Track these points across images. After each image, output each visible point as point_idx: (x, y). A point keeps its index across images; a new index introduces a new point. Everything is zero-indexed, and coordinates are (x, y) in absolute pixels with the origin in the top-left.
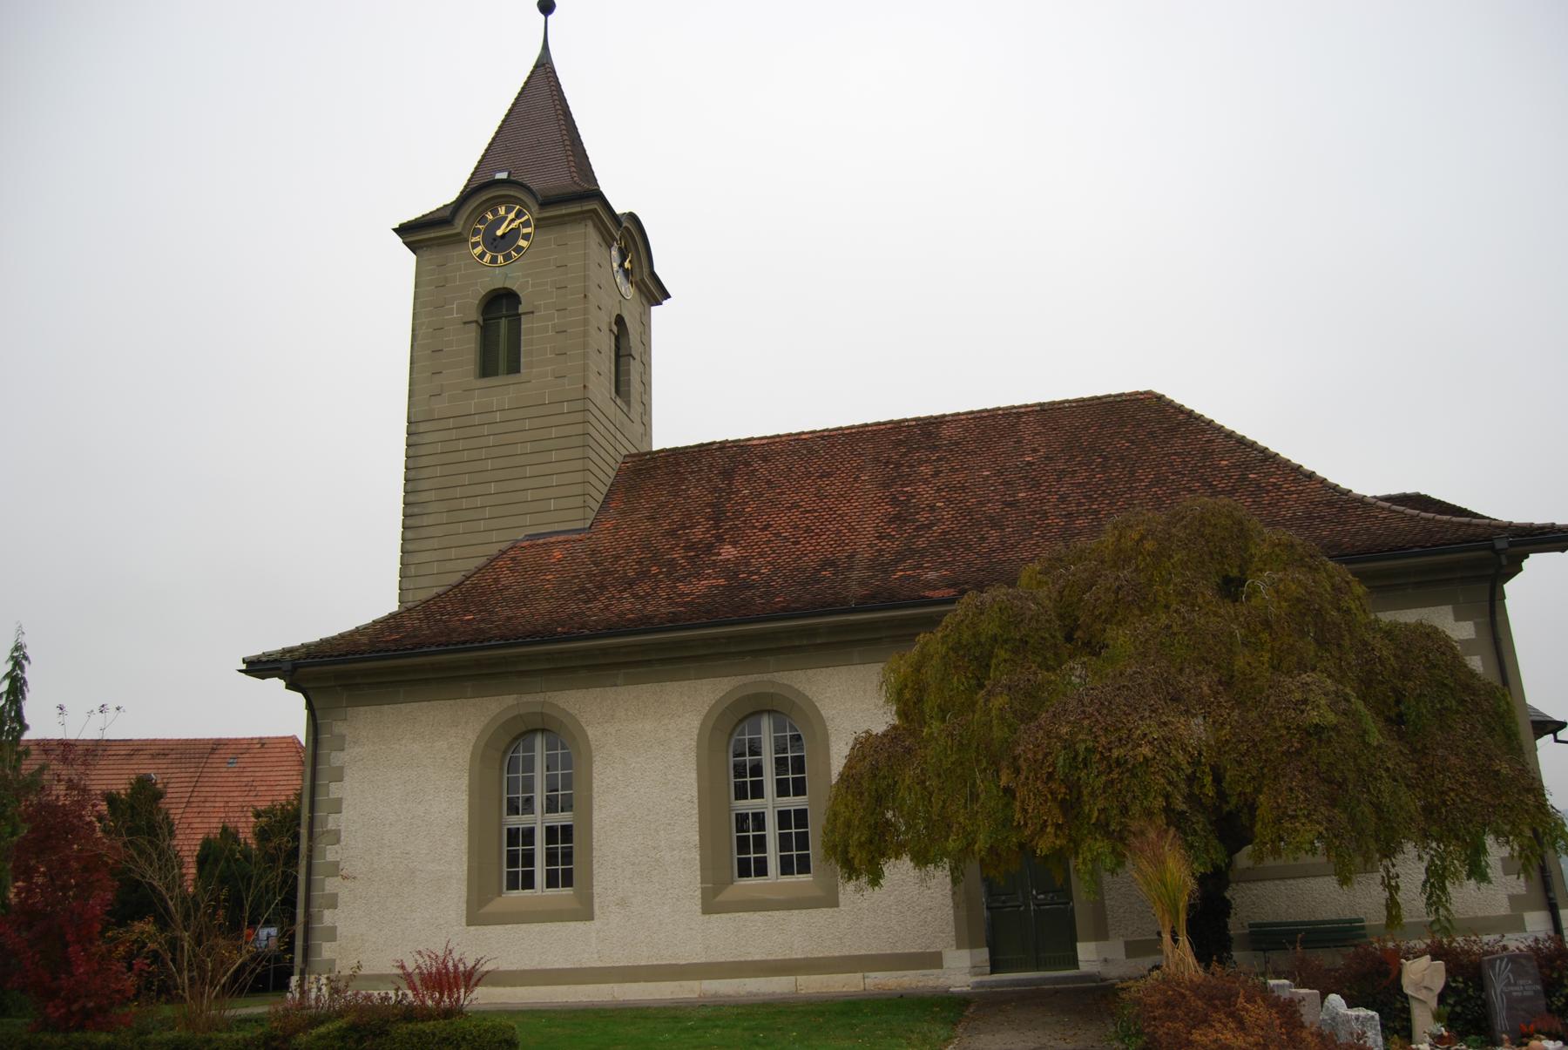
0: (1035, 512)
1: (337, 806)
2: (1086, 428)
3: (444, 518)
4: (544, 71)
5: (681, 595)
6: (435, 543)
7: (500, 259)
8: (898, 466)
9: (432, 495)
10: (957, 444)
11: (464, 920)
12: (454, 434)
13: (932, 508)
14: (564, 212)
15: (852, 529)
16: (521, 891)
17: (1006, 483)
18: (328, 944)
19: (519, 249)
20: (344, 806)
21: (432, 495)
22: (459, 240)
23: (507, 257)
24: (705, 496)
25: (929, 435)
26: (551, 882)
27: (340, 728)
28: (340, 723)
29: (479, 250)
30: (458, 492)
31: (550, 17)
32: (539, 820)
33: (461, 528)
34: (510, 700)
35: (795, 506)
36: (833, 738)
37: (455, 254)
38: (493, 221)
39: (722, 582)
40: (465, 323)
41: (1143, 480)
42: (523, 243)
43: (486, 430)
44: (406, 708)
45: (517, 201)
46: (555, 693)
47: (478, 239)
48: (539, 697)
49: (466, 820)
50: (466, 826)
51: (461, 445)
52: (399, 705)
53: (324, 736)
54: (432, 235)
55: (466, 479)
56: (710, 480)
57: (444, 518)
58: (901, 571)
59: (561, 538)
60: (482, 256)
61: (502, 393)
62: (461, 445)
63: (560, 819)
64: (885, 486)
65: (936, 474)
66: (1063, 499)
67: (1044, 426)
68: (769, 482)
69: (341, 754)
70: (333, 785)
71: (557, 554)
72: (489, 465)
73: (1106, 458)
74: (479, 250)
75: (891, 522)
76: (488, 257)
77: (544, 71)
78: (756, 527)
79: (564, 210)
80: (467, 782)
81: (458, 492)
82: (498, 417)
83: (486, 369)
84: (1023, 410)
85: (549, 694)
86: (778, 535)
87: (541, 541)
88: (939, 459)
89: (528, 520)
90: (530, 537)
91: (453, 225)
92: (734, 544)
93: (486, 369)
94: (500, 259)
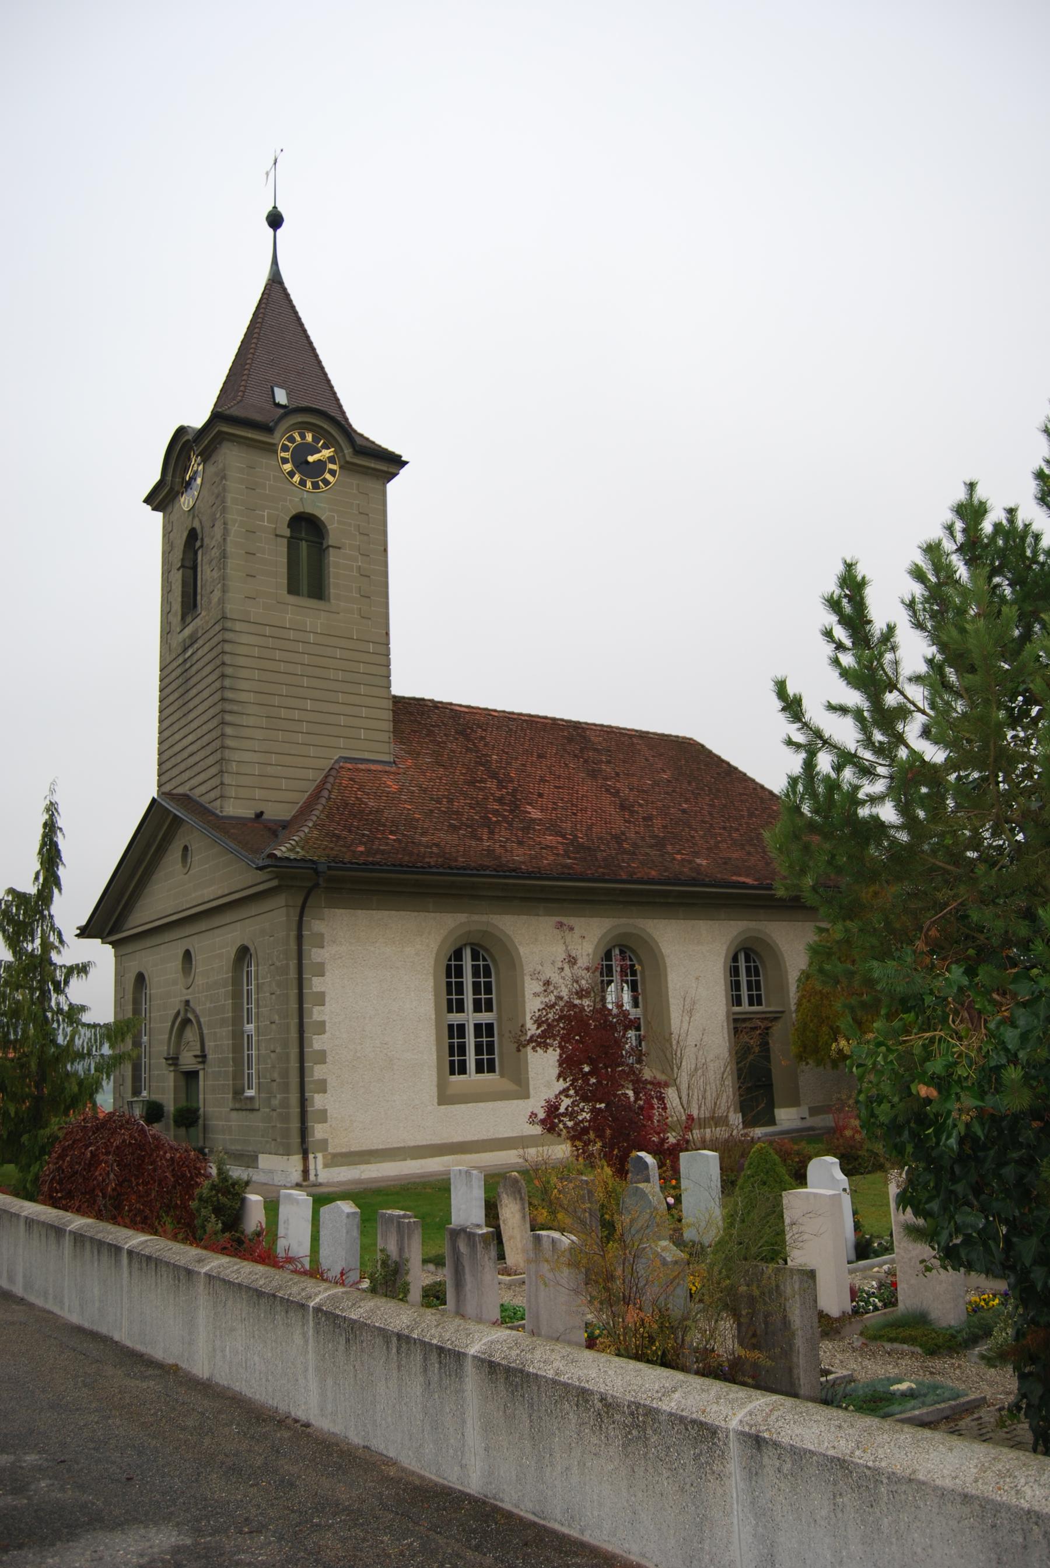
1: (320, 999)
3: (264, 722)
4: (275, 286)
7: (309, 484)
9: (251, 697)
11: (436, 1100)
14: (373, 465)
16: (486, 1074)
18: (320, 1125)
19: (326, 482)
20: (327, 999)
21: (251, 697)
22: (270, 449)
23: (315, 486)
26: (479, 1069)
28: (318, 922)
29: (288, 467)
30: (276, 701)
31: (279, 231)
32: (470, 1018)
34: (462, 917)
36: (669, 969)
37: (264, 461)
38: (308, 444)
40: (277, 535)
42: (328, 476)
43: (301, 647)
44: (377, 914)
45: (326, 434)
46: (496, 916)
47: (286, 455)
48: (484, 918)
49: (433, 1017)
50: (433, 1022)
51: (278, 655)
52: (371, 912)
54: (250, 435)
55: (284, 690)
57: (264, 722)
59: (379, 767)
60: (291, 474)
62: (278, 655)
63: (456, 1018)
69: (319, 950)
70: (315, 979)
74: (288, 467)
76: (297, 478)
77: (275, 286)
79: (373, 464)
80: (432, 984)
81: (276, 701)
82: (312, 638)
85: (491, 916)
89: (341, 743)
90: (347, 759)
91: (273, 434)
94: (309, 484)
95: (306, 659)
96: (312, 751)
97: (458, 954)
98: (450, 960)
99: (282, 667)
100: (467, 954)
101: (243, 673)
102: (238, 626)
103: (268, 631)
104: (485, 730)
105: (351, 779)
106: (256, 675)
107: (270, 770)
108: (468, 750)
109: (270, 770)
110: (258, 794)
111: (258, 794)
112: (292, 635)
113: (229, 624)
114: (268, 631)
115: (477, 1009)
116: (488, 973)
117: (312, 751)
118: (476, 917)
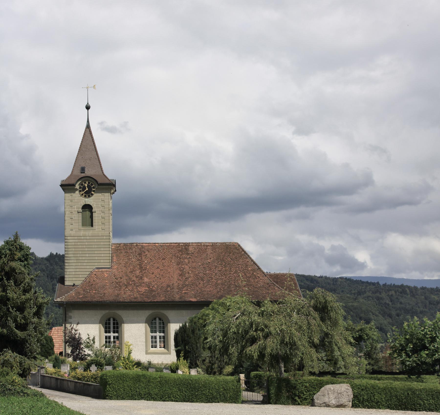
0: (210, 277)
2: (222, 253)
5: (140, 291)
6: (73, 267)
7: (87, 196)
8: (180, 258)
9: (72, 255)
10: (193, 253)
12: (77, 241)
13: (189, 273)
14: (104, 187)
15: (172, 277)
17: (204, 268)
21: (72, 255)
24: (136, 262)
25: (187, 249)
27: (70, 314)
30: (79, 255)
33: (80, 264)
34: (107, 311)
35: (158, 268)
39: (147, 288)
41: (232, 271)
43: (85, 241)
44: (85, 311)
48: (113, 311)
51: (79, 244)
53: (67, 316)
55: (81, 252)
56: (136, 257)
57: (75, 261)
58: (184, 290)
59: (105, 270)
61: (88, 232)
62: (79, 244)
64: (178, 265)
65: (189, 262)
66: (216, 274)
67: (212, 250)
68: (151, 259)
71: (106, 275)
72: (86, 249)
73: (225, 263)
75: (180, 276)
78: (150, 273)
79: (104, 187)
81: (79, 255)
82: (88, 238)
83: (84, 225)
84: (208, 244)
86: (156, 276)
87: (100, 270)
88: (189, 258)
89: (96, 264)
90: (97, 268)
92: (147, 277)
93: (84, 225)
95: (86, 244)
96: (88, 267)
97: (109, 320)
98: (107, 321)
99: (80, 246)
100: (112, 320)
101: (70, 250)
102: (69, 238)
103: (76, 238)
104: (149, 252)
105: (95, 275)
106: (73, 249)
107: (77, 273)
108: (139, 260)
109: (77, 273)
110: (74, 279)
111: (74, 279)
112: (83, 238)
113: (66, 238)
114: (76, 238)
115: (114, 332)
116: (117, 324)
117: (88, 267)
118: (111, 311)
